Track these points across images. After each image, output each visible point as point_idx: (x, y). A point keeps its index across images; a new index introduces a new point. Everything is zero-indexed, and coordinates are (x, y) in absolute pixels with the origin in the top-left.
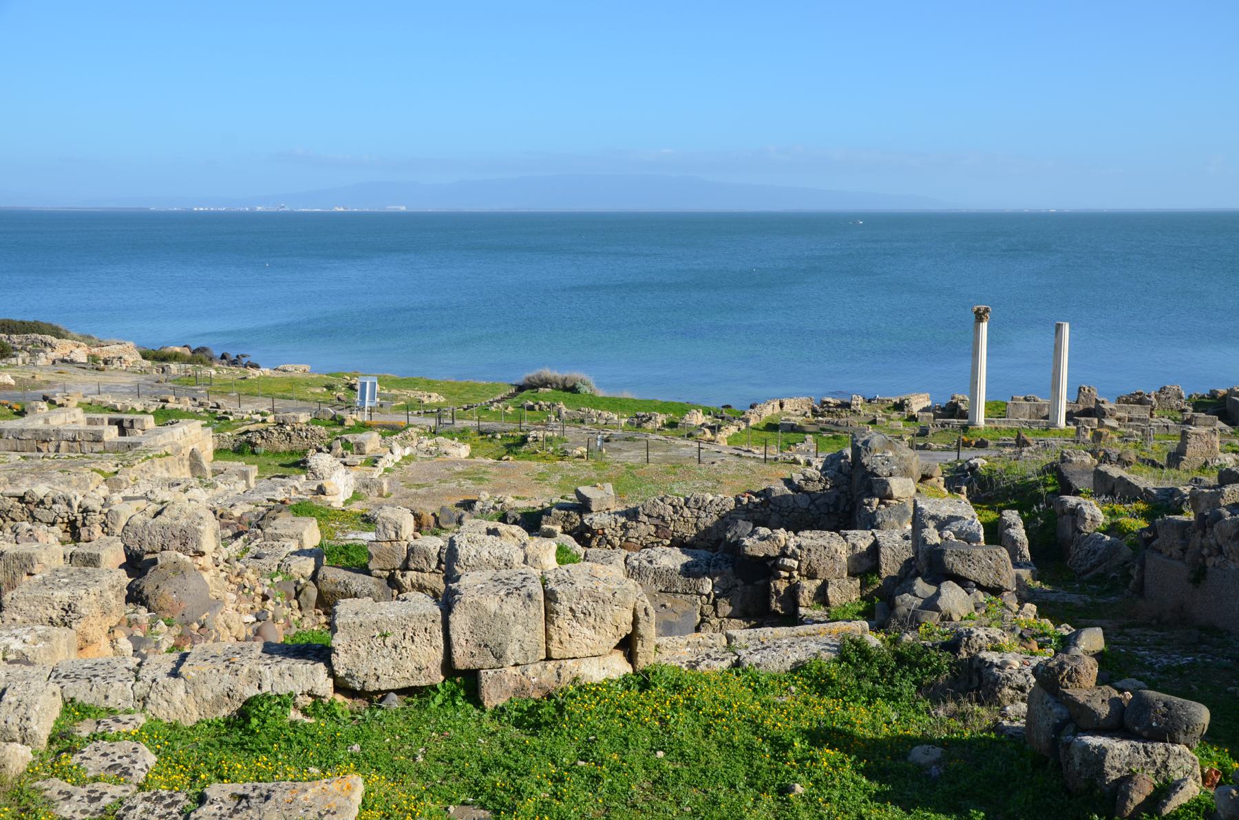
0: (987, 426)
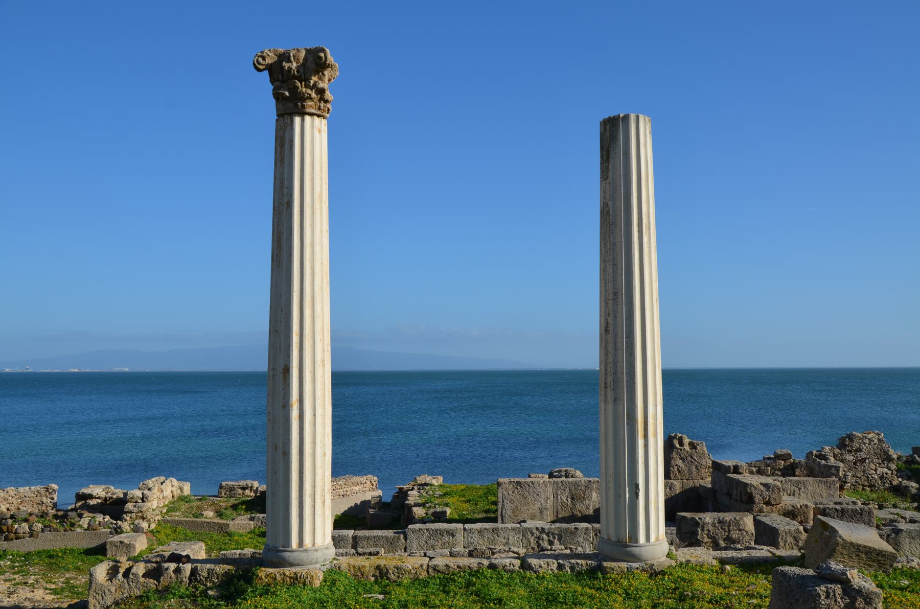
0: (344, 561)
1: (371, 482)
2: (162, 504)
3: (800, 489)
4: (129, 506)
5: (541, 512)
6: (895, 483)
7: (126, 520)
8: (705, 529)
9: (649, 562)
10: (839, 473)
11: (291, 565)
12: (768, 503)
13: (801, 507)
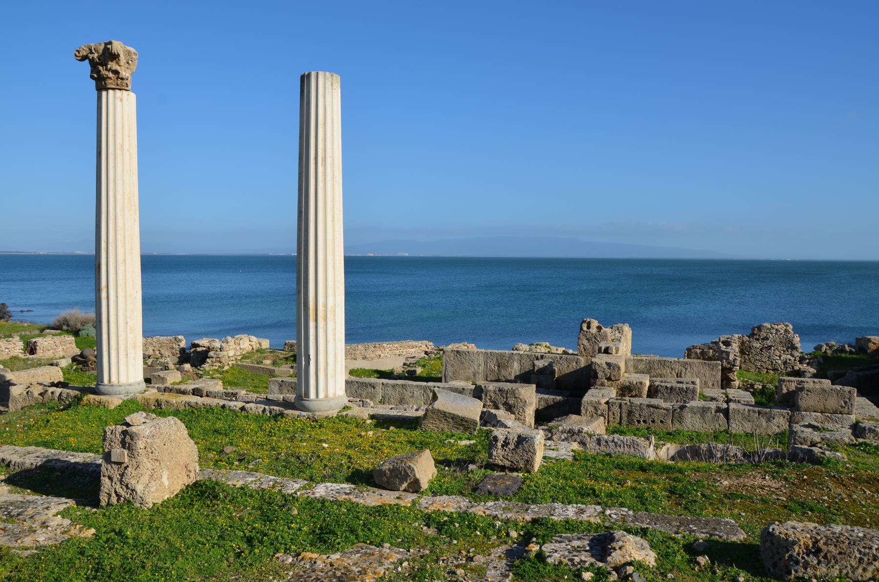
1: (426, 346)
2: (239, 354)
3: (686, 369)
4: (211, 354)
5: (474, 375)
6: (796, 368)
7: (208, 363)
8: (488, 395)
9: (320, 413)
10: (729, 357)
11: (104, 394)
12: (609, 379)
13: (637, 383)
